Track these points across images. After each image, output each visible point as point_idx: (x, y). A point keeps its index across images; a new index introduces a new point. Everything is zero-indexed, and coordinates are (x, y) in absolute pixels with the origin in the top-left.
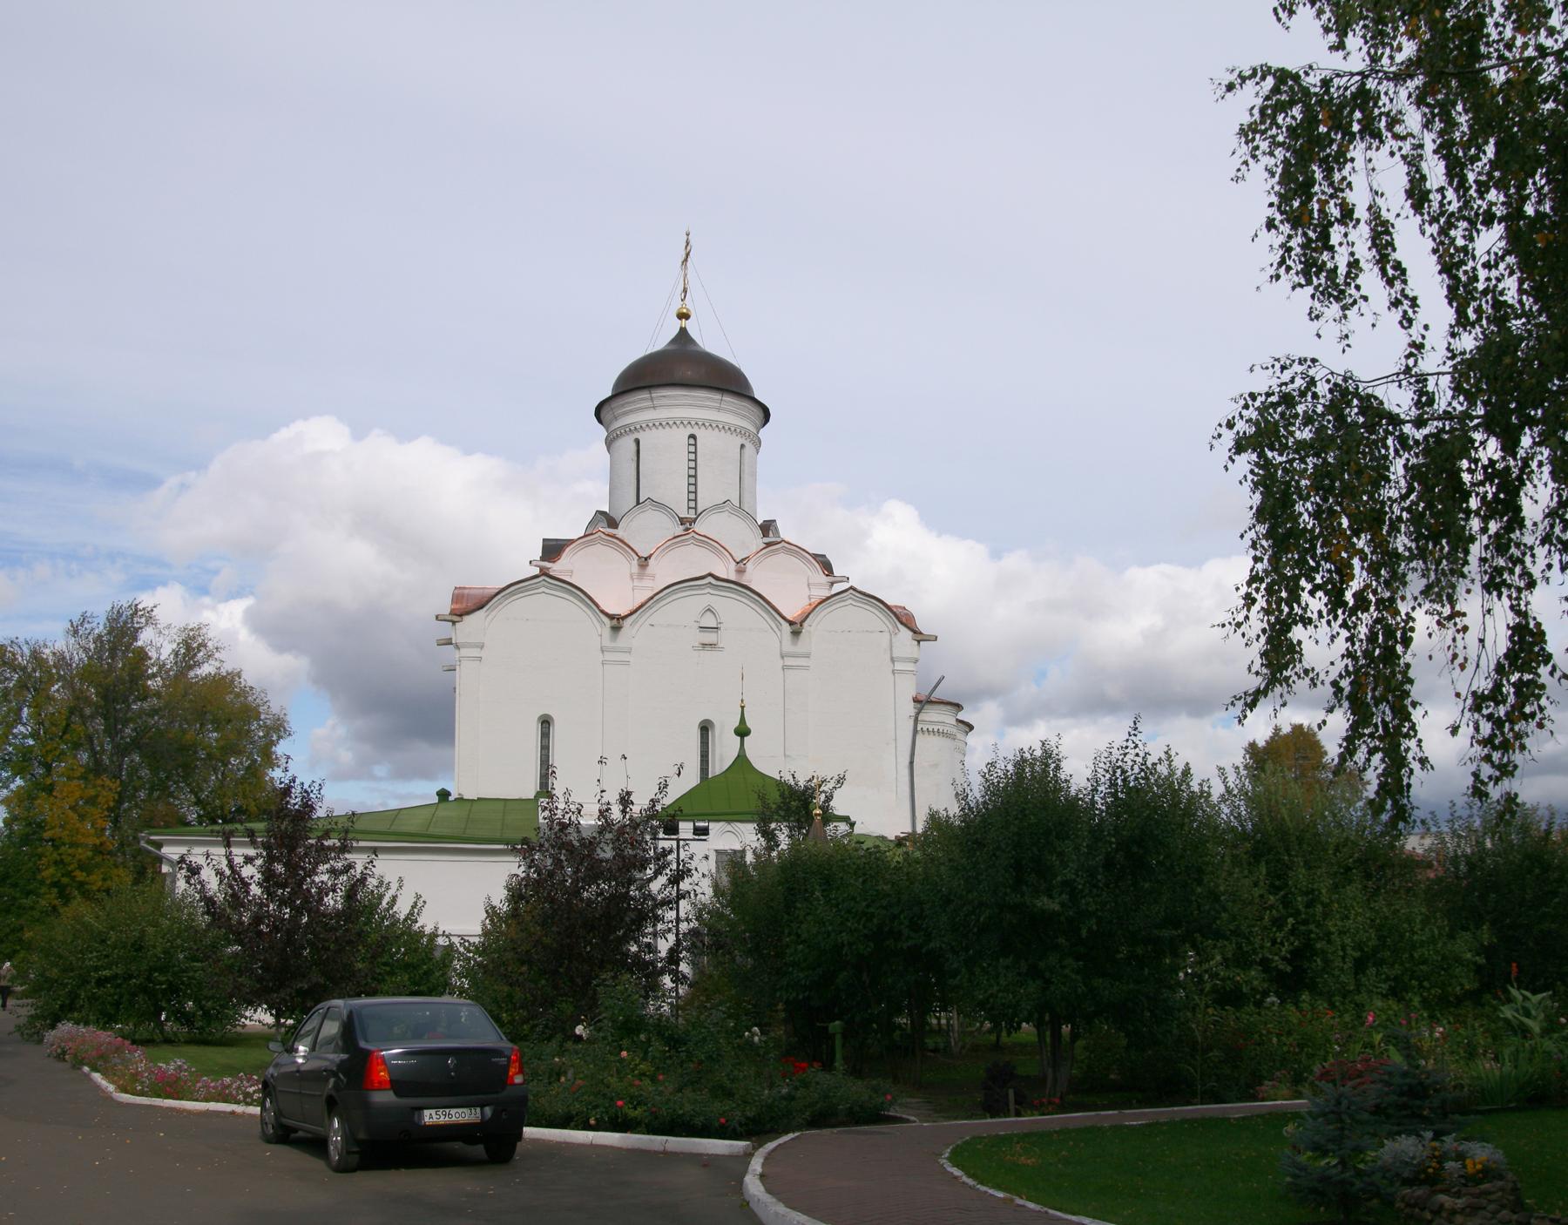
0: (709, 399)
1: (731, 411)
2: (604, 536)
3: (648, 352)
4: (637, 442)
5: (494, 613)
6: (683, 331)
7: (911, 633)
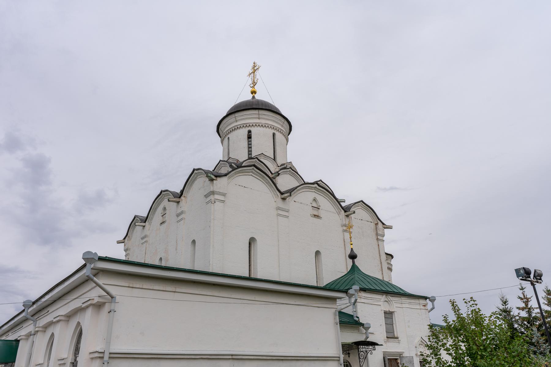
0: (280, 120)
1: (285, 129)
2: (258, 161)
4: (250, 132)
6: (254, 97)
7: (382, 224)
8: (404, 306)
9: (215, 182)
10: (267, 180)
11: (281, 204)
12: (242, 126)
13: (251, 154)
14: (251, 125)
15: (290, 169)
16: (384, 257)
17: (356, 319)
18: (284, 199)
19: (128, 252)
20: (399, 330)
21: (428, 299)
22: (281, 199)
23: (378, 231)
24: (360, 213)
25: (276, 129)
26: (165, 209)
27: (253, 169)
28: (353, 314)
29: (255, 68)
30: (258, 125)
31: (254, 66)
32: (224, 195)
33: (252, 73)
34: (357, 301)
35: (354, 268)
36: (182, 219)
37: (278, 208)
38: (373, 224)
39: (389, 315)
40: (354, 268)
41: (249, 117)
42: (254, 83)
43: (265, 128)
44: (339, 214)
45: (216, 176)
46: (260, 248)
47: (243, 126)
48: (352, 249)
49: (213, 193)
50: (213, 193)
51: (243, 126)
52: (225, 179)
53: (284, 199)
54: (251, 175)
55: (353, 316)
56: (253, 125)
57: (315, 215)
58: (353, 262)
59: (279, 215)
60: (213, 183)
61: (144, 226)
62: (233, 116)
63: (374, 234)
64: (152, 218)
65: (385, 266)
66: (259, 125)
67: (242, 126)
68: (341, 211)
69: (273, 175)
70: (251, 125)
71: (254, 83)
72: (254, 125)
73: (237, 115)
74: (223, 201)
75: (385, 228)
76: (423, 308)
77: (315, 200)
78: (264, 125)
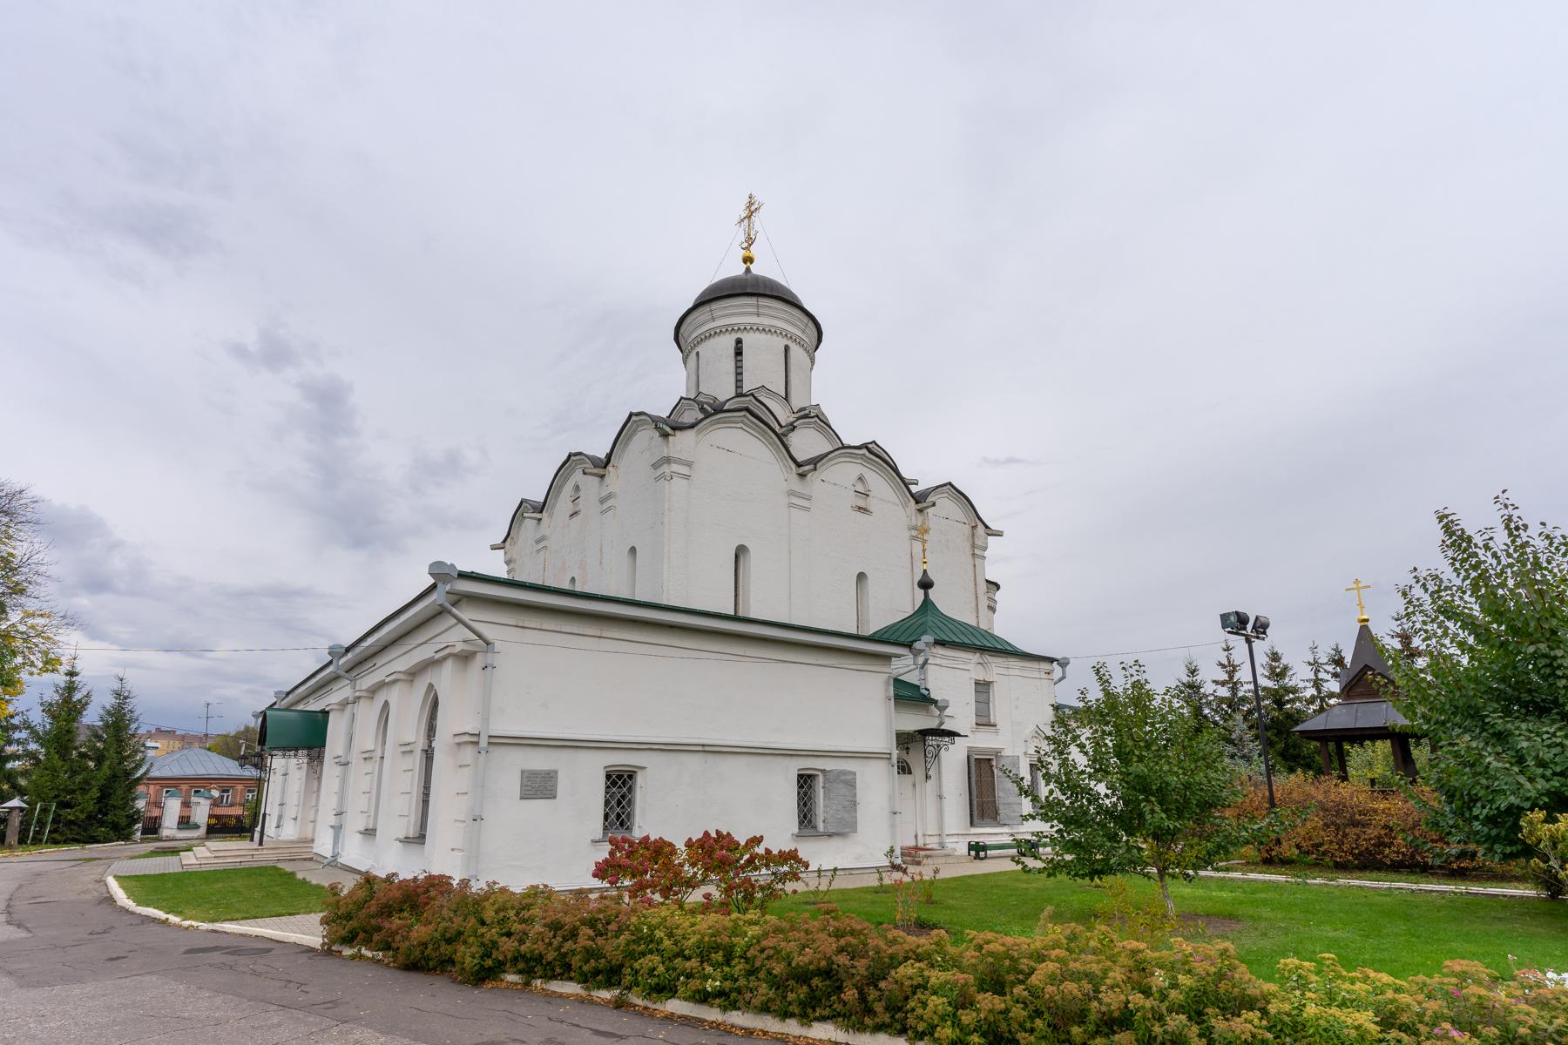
0: (802, 320)
1: (808, 337)
2: (754, 400)
3: (716, 280)
4: (739, 341)
5: (700, 437)
6: (748, 270)
8: (1011, 672)
9: (671, 438)
10: (771, 438)
11: (796, 484)
12: (724, 330)
13: (742, 387)
14: (742, 328)
15: (816, 419)
16: (983, 587)
17: (926, 693)
18: (802, 476)
19: (512, 565)
20: (998, 712)
21: (1055, 663)
22: (796, 476)
23: (976, 539)
24: (945, 506)
25: (791, 337)
26: (577, 488)
27: (744, 416)
28: (918, 684)
29: (753, 208)
30: (755, 328)
31: (751, 204)
32: (689, 464)
33: (745, 218)
34: (929, 662)
35: (927, 604)
36: (609, 509)
37: (791, 493)
38: (967, 526)
39: (983, 687)
40: (927, 604)
41: (737, 312)
42: (750, 241)
43: (769, 336)
44: (905, 506)
45: (674, 429)
46: (755, 565)
47: (727, 330)
48: (925, 571)
49: (668, 460)
50: (668, 460)
51: (727, 330)
52: (690, 434)
53: (802, 476)
54: (741, 428)
55: (918, 687)
56: (745, 328)
57: (860, 508)
58: (926, 595)
59: (791, 505)
60: (668, 441)
61: (540, 520)
62: (706, 308)
63: (968, 545)
64: (554, 505)
65: (984, 602)
66: (758, 329)
67: (724, 330)
68: (910, 501)
69: (784, 429)
70: (742, 328)
71: (750, 241)
72: (748, 328)
73: (714, 306)
74: (688, 477)
75: (989, 535)
76: (1046, 676)
77: (860, 479)
78: (767, 329)
